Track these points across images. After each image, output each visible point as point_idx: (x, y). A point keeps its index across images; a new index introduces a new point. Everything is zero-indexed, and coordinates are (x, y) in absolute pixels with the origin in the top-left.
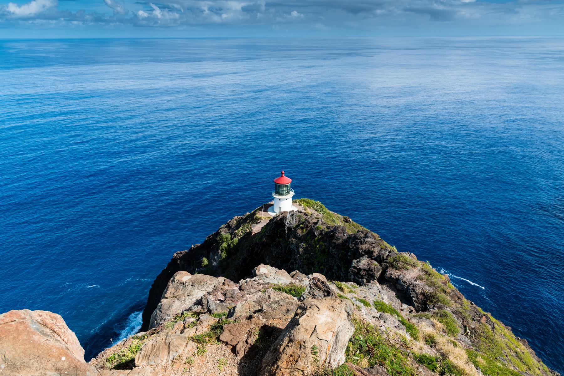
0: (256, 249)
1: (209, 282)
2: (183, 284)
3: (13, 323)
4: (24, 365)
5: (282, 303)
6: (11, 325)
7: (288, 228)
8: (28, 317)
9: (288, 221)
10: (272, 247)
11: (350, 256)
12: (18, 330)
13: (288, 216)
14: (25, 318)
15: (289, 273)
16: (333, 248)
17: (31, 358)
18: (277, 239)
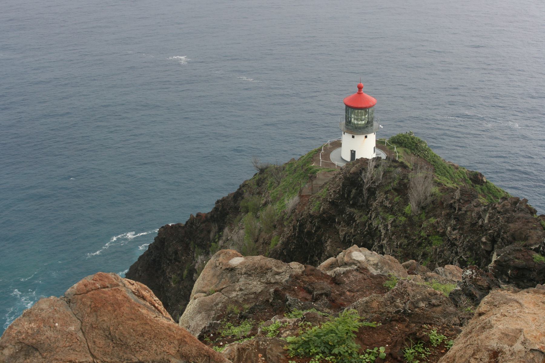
0: (308, 226)
1: (275, 269)
2: (232, 270)
3: (107, 289)
4: (139, 347)
5: (434, 301)
6: (104, 293)
7: (369, 189)
8: (120, 284)
9: (369, 175)
10: (339, 223)
11: (484, 243)
12: (117, 300)
13: (371, 166)
14: (118, 285)
15: (401, 263)
16: (454, 229)
17: (146, 338)
18: (348, 210)
